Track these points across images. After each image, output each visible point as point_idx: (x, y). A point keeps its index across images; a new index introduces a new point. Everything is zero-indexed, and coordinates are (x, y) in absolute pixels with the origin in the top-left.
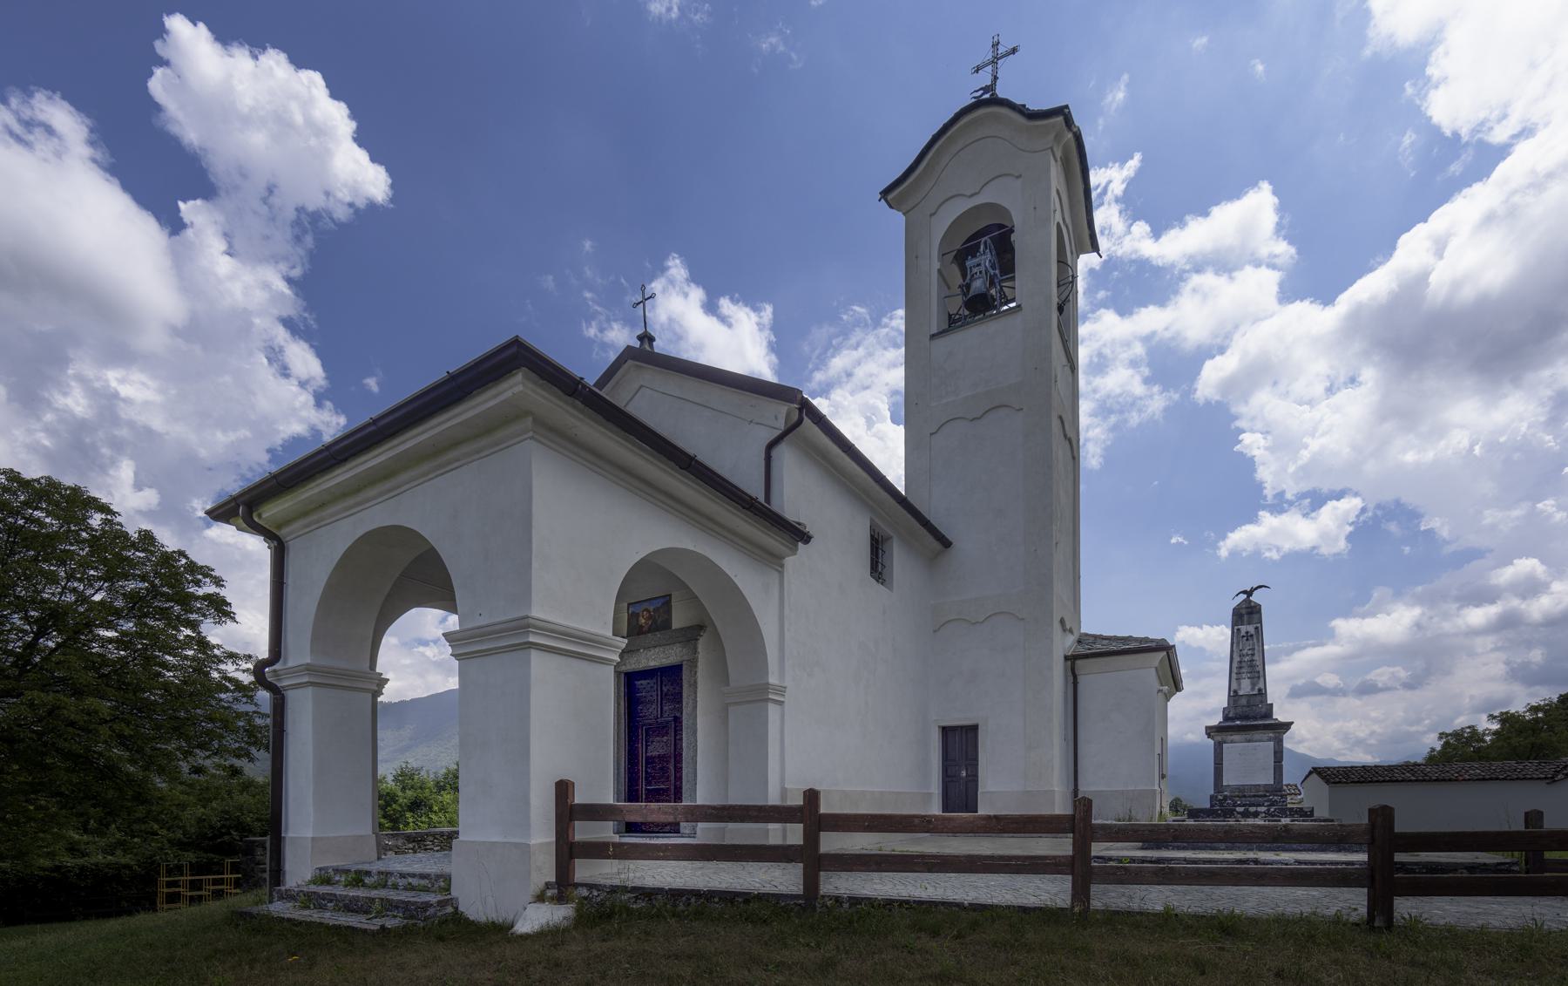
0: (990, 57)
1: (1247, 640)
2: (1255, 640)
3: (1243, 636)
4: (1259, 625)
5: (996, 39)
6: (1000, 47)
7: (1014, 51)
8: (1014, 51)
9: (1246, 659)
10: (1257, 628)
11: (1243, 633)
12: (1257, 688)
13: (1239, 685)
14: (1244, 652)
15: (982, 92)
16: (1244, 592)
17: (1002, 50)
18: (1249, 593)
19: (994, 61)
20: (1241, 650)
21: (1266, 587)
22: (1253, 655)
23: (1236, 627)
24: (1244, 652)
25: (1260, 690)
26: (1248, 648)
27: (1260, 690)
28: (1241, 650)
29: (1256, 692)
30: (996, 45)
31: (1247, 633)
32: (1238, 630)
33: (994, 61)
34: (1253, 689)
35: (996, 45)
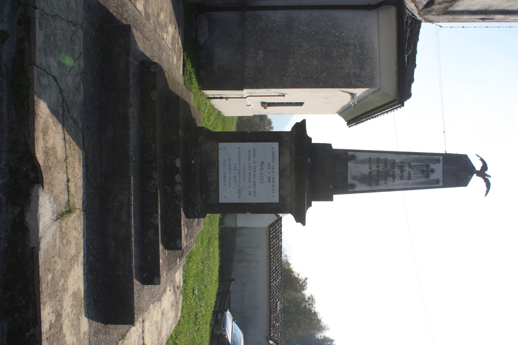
3: (428, 166)
11: (432, 166)
14: (407, 168)
16: (485, 167)
18: (483, 173)
20: (409, 163)
22: (402, 178)
23: (441, 158)
24: (407, 168)
26: (412, 172)
29: (350, 181)
31: (433, 171)
34: (354, 178)
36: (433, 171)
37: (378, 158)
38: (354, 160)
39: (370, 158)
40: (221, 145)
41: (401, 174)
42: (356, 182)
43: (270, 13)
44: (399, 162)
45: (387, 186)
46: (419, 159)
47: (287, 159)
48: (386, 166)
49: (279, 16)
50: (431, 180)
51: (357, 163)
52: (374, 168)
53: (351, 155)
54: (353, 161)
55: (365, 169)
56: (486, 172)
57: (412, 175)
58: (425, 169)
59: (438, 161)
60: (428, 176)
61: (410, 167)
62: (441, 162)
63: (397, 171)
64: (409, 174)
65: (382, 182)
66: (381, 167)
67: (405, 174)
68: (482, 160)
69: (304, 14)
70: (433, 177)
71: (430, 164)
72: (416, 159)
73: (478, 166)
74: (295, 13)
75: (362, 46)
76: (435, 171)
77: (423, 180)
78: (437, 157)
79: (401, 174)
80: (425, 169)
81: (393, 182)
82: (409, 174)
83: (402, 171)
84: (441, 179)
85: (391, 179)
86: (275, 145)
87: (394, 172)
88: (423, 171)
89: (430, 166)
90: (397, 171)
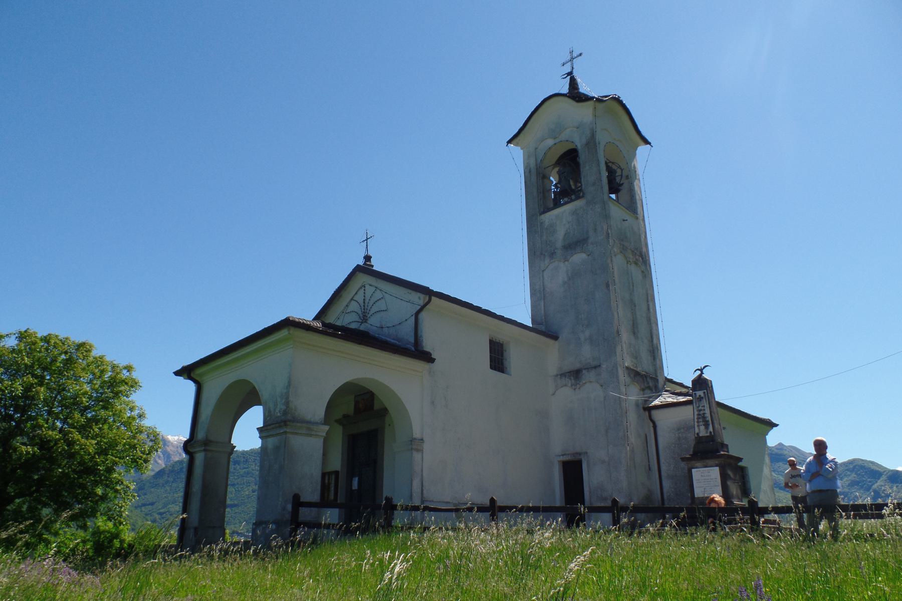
0: (569, 58)
2: (704, 400)
3: (698, 398)
4: (705, 391)
5: (571, 49)
6: (573, 53)
7: (581, 55)
8: (581, 55)
10: (704, 393)
11: (698, 396)
12: (709, 431)
13: (699, 429)
14: (700, 408)
15: (566, 75)
17: (575, 55)
18: (701, 370)
19: (572, 59)
21: (707, 366)
22: (704, 410)
25: (711, 432)
27: (711, 432)
29: (708, 434)
30: (571, 52)
31: (700, 396)
32: (695, 394)
33: (572, 59)
34: (707, 433)
35: (571, 52)
36: (700, 396)
40: (696, 496)
42: (709, 431)
43: (665, 490)
47: (698, 464)
48: (699, 418)
49: (666, 484)
51: (700, 432)
52: (701, 423)
55: (702, 428)
60: (702, 398)
61: (699, 407)
62: (696, 392)
63: (701, 412)
64: (702, 406)
65: (707, 419)
66: (701, 420)
67: (702, 408)
68: (695, 371)
69: (664, 468)
70: (702, 395)
73: (699, 373)
74: (664, 474)
75: (679, 429)
77: (704, 400)
82: (702, 406)
83: (701, 410)
84: (703, 391)
85: (705, 415)
88: (700, 400)
90: (701, 412)
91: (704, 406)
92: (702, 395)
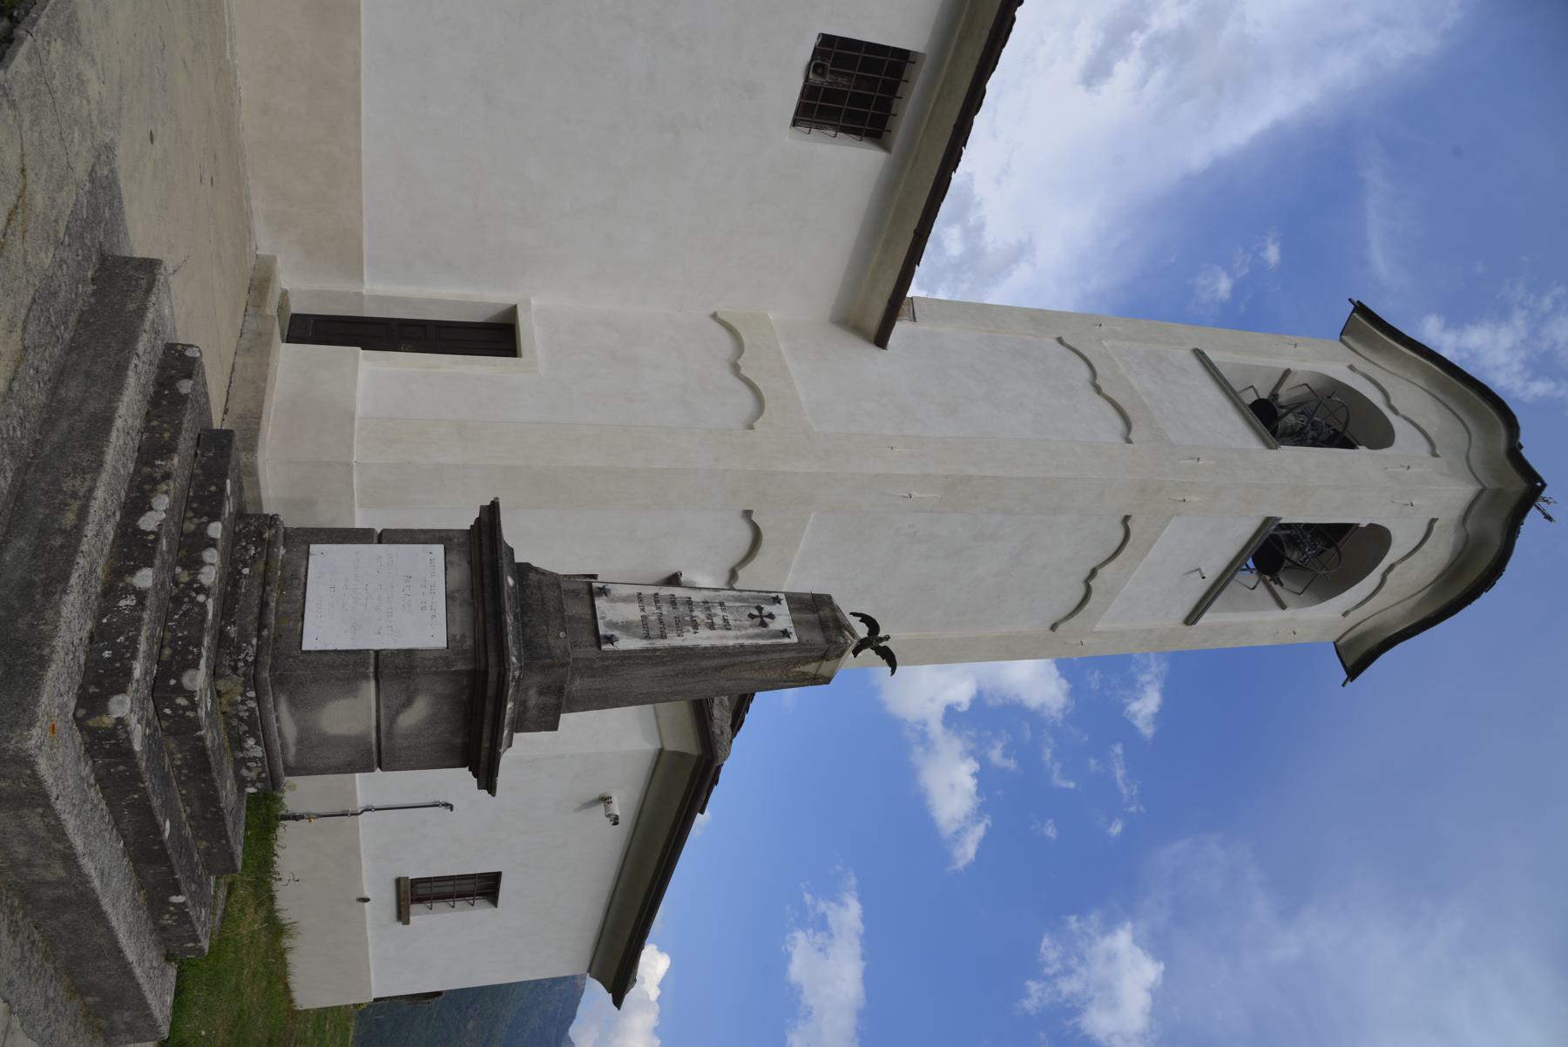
1: (751, 616)
2: (751, 631)
3: (760, 609)
7: (1549, 518)
8: (1549, 518)
9: (699, 615)
10: (785, 633)
12: (616, 633)
14: (717, 610)
22: (712, 626)
24: (717, 610)
26: (730, 618)
27: (610, 639)
28: (721, 604)
29: (603, 631)
31: (771, 616)
37: (657, 594)
38: (606, 595)
39: (640, 594)
40: (314, 548)
41: (710, 621)
44: (699, 600)
45: (683, 640)
46: (739, 596)
50: (772, 631)
51: (612, 600)
53: (599, 588)
54: (604, 597)
55: (632, 612)
56: (879, 635)
57: (731, 622)
58: (756, 613)
59: (776, 600)
62: (784, 602)
64: (725, 620)
67: (718, 621)
68: (866, 619)
70: (775, 626)
71: (762, 606)
72: (733, 596)
76: (777, 617)
78: (774, 595)
79: (710, 621)
80: (756, 613)
81: (695, 633)
82: (725, 620)
85: (691, 629)
86: (439, 549)
87: (692, 617)
89: (762, 608)
91: (727, 626)
92: (775, 626)
